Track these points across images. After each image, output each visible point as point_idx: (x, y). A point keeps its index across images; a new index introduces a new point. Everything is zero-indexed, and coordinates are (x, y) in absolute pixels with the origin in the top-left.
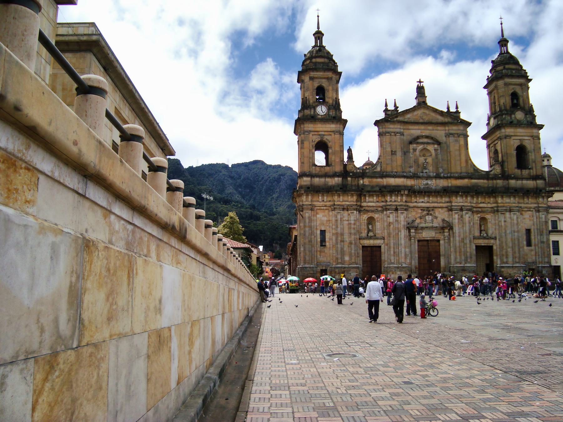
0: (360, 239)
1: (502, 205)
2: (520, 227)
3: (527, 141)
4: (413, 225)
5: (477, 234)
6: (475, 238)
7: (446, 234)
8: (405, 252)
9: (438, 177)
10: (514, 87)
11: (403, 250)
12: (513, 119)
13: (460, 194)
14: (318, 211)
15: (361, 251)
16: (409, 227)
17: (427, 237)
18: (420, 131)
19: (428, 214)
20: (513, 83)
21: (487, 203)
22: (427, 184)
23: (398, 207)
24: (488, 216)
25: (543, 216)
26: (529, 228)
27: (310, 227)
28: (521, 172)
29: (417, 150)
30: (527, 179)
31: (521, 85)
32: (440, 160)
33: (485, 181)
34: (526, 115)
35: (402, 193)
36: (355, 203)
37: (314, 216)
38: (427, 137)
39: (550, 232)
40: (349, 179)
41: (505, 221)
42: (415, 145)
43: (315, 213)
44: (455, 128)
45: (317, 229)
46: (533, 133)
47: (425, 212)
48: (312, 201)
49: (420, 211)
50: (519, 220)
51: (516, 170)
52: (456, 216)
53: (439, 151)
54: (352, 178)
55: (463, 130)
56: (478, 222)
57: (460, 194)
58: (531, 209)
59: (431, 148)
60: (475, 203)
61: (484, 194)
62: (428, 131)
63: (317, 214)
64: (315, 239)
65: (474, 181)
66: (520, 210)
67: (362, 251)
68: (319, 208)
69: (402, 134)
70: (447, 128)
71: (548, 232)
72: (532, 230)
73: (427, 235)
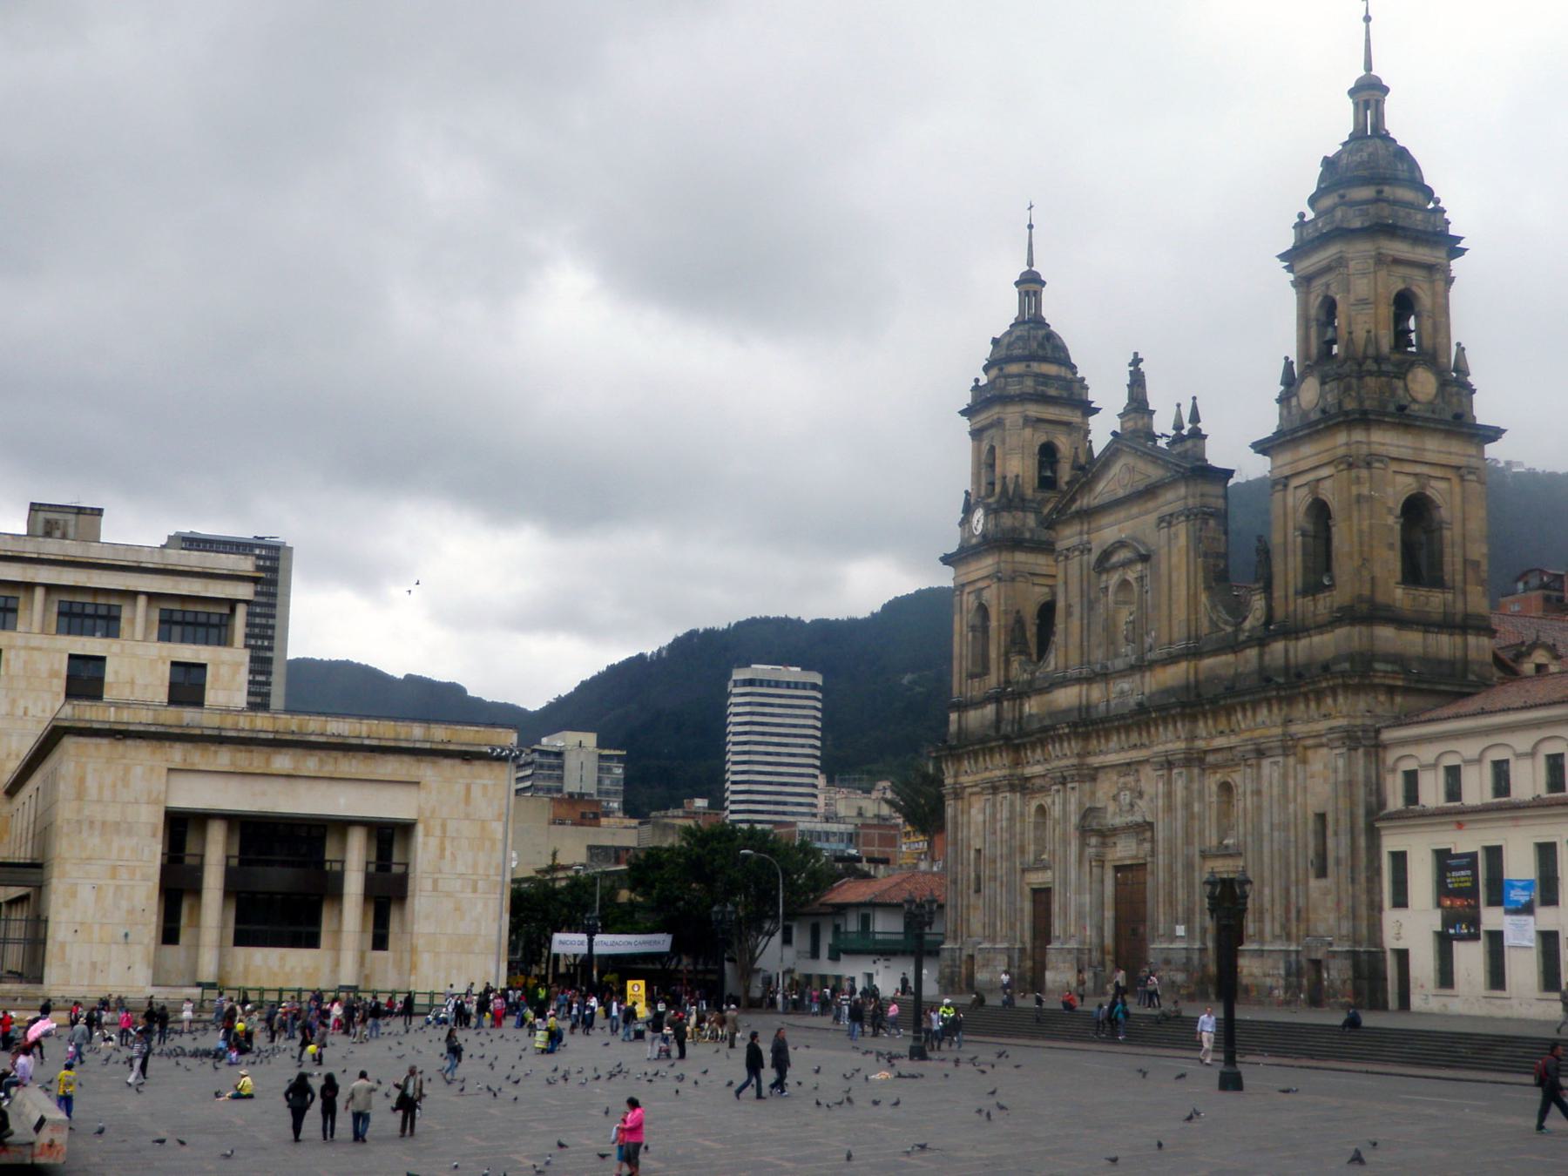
0: (1023, 871)
1: (1247, 735)
2: (1291, 807)
3: (1327, 484)
4: (1095, 826)
5: (1214, 842)
6: (1204, 855)
7: (1147, 846)
8: (1081, 906)
9: (1141, 666)
10: (1323, 280)
11: (1073, 898)
12: (1294, 411)
13: (1154, 715)
14: (973, 798)
15: (1028, 906)
16: (1092, 828)
17: (1125, 858)
18: (1116, 528)
19: (1125, 787)
20: (1312, 269)
21: (1211, 736)
22: (1122, 692)
23: (1065, 774)
24: (1236, 778)
25: (1341, 763)
26: (1321, 811)
27: (955, 843)
28: (1314, 600)
29: (1110, 590)
30: (1321, 628)
31: (1328, 269)
32: (1150, 610)
33: (1230, 658)
34: (1323, 383)
35: (1061, 732)
36: (1006, 772)
37: (962, 812)
38: (1121, 544)
39: (1376, 817)
40: (1005, 703)
41: (1252, 792)
42: (1104, 577)
43: (966, 807)
44: (1170, 495)
45: (969, 847)
46: (1335, 448)
47: (1122, 780)
48: (956, 775)
49: (1115, 778)
50: (1291, 783)
51: (1300, 601)
52: (1160, 785)
53: (1148, 580)
54: (1008, 700)
55: (1185, 498)
56: (1214, 799)
57: (1154, 715)
58: (1324, 740)
59: (1131, 575)
60: (1205, 739)
61: (1207, 707)
62: (1129, 524)
63: (970, 806)
64: (965, 873)
65: (1208, 662)
66: (1290, 746)
67: (1035, 902)
68: (969, 790)
69: (1085, 549)
70: (1161, 500)
71: (1361, 823)
72: (1330, 819)
73: (1124, 850)
